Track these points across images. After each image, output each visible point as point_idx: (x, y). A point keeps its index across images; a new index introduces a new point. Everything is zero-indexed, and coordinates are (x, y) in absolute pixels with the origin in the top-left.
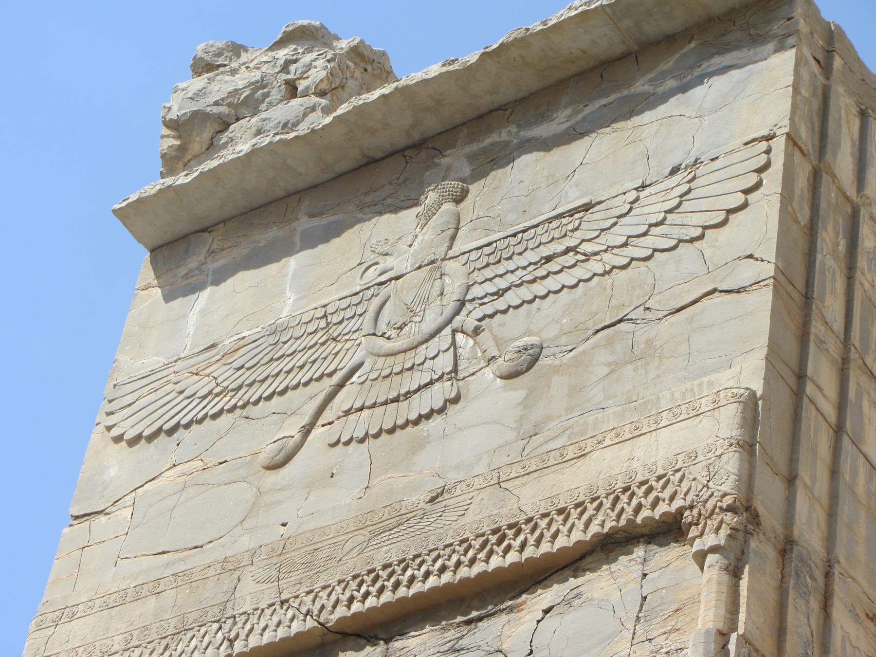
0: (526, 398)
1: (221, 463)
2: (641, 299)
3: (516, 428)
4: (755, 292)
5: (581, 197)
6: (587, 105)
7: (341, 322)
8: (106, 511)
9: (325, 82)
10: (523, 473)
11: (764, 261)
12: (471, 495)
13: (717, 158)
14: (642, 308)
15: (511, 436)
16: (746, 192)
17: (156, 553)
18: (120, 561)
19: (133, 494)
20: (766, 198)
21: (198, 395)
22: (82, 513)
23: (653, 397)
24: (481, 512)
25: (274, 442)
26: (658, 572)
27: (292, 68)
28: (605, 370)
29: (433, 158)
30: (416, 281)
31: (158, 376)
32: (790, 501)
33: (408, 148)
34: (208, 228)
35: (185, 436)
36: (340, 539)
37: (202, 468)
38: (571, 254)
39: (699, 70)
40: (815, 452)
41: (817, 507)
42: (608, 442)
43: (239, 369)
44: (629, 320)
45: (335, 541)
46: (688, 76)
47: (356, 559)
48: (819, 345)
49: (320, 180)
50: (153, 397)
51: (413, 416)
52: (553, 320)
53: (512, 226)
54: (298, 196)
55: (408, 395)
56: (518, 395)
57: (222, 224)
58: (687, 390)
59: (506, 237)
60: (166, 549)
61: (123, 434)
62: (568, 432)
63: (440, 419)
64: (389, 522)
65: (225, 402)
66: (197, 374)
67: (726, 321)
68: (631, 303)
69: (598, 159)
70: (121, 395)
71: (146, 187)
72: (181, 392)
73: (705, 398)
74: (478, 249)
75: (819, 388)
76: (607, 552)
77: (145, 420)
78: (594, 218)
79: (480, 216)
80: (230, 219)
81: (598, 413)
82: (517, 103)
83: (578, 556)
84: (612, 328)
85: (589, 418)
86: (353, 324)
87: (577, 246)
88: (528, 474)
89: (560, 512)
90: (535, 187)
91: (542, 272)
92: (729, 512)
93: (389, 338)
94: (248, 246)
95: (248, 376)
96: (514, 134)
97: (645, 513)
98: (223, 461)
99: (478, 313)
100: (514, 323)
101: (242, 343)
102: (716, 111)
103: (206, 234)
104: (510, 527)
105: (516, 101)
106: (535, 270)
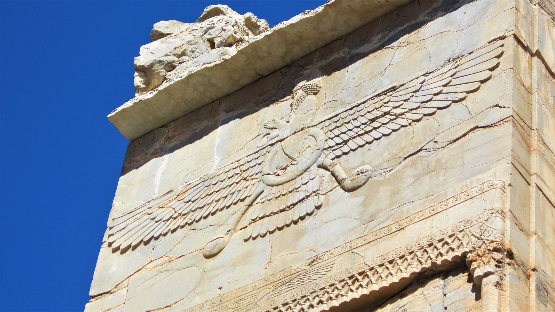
0: (364, 201)
1: (180, 257)
3: (359, 219)
4: (502, 125)
5: (389, 84)
6: (390, 32)
9: (231, 38)
10: (365, 243)
11: (504, 107)
12: (334, 258)
13: (472, 52)
14: (432, 142)
15: (356, 223)
16: (492, 69)
19: (127, 280)
20: (504, 71)
23: (443, 192)
24: (341, 268)
25: (211, 241)
28: (412, 180)
30: (293, 141)
33: (283, 67)
34: (165, 125)
35: (157, 244)
37: (168, 261)
38: (386, 116)
43: (188, 202)
49: (231, 91)
52: (378, 154)
54: (218, 102)
57: (174, 122)
58: (463, 186)
59: (346, 111)
61: (120, 246)
62: (391, 217)
63: (312, 219)
65: (181, 221)
66: (162, 208)
68: (425, 140)
70: (117, 224)
73: (476, 188)
74: (330, 119)
77: (132, 237)
78: (400, 95)
79: (329, 101)
81: (409, 205)
82: (348, 35)
84: (414, 155)
85: (404, 208)
86: (257, 169)
87: (389, 112)
88: (368, 243)
89: (391, 262)
90: (362, 81)
91: (368, 128)
93: (278, 175)
95: (194, 206)
96: (347, 53)
98: (181, 255)
101: (189, 188)
103: (164, 128)
104: (360, 274)
105: (347, 34)
106: (365, 127)
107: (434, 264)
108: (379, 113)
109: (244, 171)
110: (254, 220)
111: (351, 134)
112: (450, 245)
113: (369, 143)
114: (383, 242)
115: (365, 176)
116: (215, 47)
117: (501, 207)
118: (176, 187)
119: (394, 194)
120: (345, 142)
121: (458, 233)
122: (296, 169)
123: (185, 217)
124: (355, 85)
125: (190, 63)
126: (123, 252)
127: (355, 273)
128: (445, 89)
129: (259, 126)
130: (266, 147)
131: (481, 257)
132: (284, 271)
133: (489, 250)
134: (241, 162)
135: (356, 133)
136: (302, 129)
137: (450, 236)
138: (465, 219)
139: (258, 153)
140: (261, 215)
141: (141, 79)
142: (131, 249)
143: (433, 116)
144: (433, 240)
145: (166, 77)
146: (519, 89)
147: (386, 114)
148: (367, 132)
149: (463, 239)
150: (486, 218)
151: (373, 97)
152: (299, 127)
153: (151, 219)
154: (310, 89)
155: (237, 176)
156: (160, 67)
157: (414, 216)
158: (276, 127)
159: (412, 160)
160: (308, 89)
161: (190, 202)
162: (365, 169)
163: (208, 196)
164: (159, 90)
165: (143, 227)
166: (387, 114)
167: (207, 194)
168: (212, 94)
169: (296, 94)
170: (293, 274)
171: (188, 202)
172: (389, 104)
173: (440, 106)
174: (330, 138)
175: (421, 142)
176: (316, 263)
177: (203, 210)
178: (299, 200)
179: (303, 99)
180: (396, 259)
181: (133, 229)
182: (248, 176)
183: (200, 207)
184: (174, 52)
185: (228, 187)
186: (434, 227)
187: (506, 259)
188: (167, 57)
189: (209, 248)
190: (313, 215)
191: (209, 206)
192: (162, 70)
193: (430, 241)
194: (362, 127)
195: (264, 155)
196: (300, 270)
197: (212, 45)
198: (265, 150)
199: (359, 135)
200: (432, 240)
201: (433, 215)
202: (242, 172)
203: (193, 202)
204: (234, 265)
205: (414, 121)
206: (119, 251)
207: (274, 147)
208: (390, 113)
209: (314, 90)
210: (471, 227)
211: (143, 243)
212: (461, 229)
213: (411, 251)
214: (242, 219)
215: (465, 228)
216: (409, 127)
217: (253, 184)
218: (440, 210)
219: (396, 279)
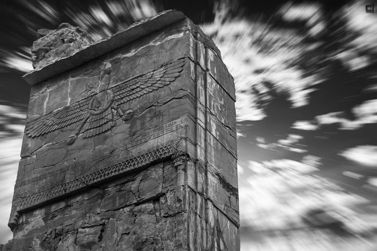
5: (139, 73)
7: (83, 106)
8: (30, 156)
9: (71, 40)
11: (185, 90)
12: (120, 152)
14: (157, 103)
15: (128, 136)
16: (179, 72)
18: (35, 169)
21: (49, 125)
27: (63, 35)
28: (149, 119)
29: (101, 62)
31: (38, 120)
32: (196, 150)
36: (89, 163)
38: (138, 88)
40: (201, 137)
41: (202, 150)
42: (152, 138)
43: (59, 118)
50: (38, 126)
51: (104, 131)
55: (102, 125)
56: (129, 125)
59: (122, 84)
60: (46, 166)
62: (142, 135)
65: (56, 127)
66: (48, 120)
72: (45, 125)
75: (201, 121)
86: (86, 107)
87: (139, 86)
89: (142, 156)
91: (131, 93)
93: (95, 110)
97: (163, 156)
99: (117, 104)
100: (126, 107)
103: (46, 82)
104: (130, 160)
111: (124, 95)
125: (54, 50)
126: (34, 138)
127: (128, 159)
137: (165, 147)
147: (138, 87)
171: (59, 118)
172: (139, 83)
199: (127, 96)
204: (80, 149)
219: (144, 164)
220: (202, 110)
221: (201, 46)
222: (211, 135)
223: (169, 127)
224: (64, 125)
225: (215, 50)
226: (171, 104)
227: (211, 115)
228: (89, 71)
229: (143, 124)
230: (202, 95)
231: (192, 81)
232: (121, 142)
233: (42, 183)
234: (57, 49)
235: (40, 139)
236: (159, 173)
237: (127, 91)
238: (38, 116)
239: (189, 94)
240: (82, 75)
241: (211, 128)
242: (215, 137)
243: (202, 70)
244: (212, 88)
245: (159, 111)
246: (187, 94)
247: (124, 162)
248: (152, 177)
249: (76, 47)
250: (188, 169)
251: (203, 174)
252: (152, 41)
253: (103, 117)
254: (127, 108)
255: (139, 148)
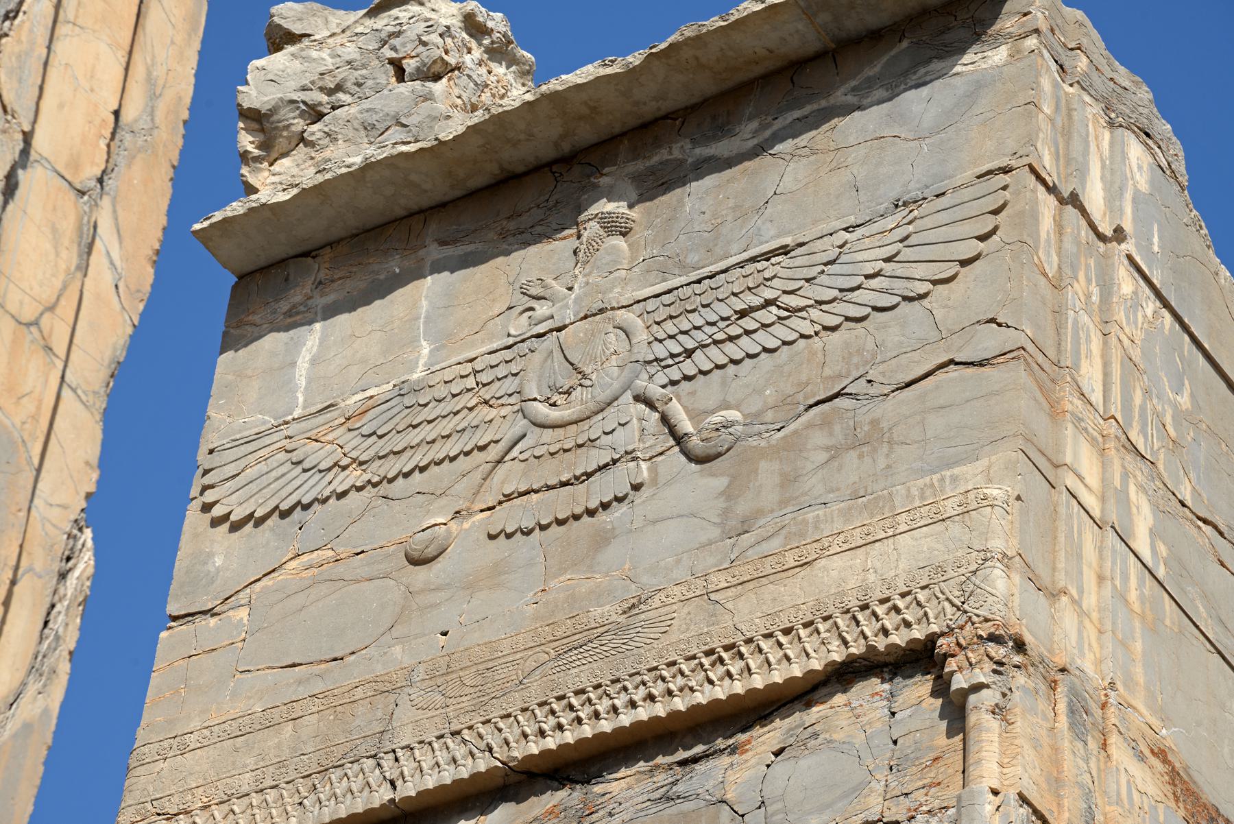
0: (728, 487)
1: (357, 554)
2: (861, 369)
3: (720, 524)
4: (1002, 366)
5: (778, 236)
6: (776, 118)
8: (215, 611)
11: (1009, 327)
12: (675, 607)
13: (943, 194)
14: (863, 380)
15: (715, 533)
17: (284, 665)
19: (248, 590)
20: (1007, 247)
22: (183, 612)
24: (688, 629)
25: (423, 530)
26: (908, 710)
28: (822, 456)
29: (589, 176)
30: (581, 335)
31: (267, 441)
33: (556, 161)
36: (518, 656)
37: (334, 560)
39: (914, 77)
43: (370, 436)
44: (847, 394)
45: (513, 659)
46: (900, 86)
47: (539, 682)
48: (1077, 424)
49: (446, 199)
50: (262, 467)
53: (695, 269)
54: (422, 217)
58: (925, 485)
60: (297, 661)
61: (230, 513)
62: (784, 531)
63: (625, 509)
64: (577, 637)
65: (356, 476)
66: (316, 441)
67: (968, 401)
69: (794, 189)
70: (221, 464)
71: (234, 204)
73: (952, 499)
76: (844, 683)
78: (796, 264)
80: (338, 241)
81: (818, 510)
82: (689, 111)
83: (809, 686)
84: (827, 404)
85: (809, 515)
86: (510, 385)
87: (776, 299)
89: (787, 632)
90: (719, 221)
91: (734, 330)
92: (992, 642)
93: (554, 405)
94: (364, 278)
96: (688, 151)
98: (359, 550)
99: (662, 378)
102: (938, 133)
103: (309, 260)
104: (727, 648)
105: (686, 108)
106: (727, 326)
107: (871, 649)
108: (756, 301)
109: (484, 385)
110: (509, 497)
112: (903, 613)
113: (735, 362)
114: (771, 586)
115: (731, 434)
116: (406, 79)
117: (1002, 548)
118: (342, 398)
119: (788, 480)
120: (689, 353)
121: (918, 590)
122: (589, 396)
123: (364, 467)
124: (706, 229)
125: (354, 110)
126: (236, 527)
127: (716, 644)
128: (889, 268)
129: (511, 286)
130: (528, 338)
131: (965, 648)
132: (573, 620)
133: (980, 637)
134: (478, 365)
135: (710, 337)
136: (602, 311)
137: (903, 595)
138: (931, 563)
139: (510, 350)
140: (522, 488)
141: (251, 139)
142: (252, 523)
143: (864, 324)
144: (868, 597)
145: (305, 135)
146: (1036, 285)
147: (769, 303)
148: (731, 339)
149: (928, 605)
150: (973, 567)
151: (742, 262)
152: (595, 305)
153: (293, 463)
154: (614, 224)
155: (470, 394)
156: (292, 115)
157: (830, 539)
158: (547, 296)
159: (823, 414)
160: (609, 223)
161: (374, 437)
162: (730, 419)
163: (411, 428)
164: (303, 189)
165: (277, 479)
166: (772, 305)
167: (409, 423)
168: (411, 201)
169: (585, 229)
170: (592, 629)
171: (370, 436)
172: (775, 283)
173: (879, 305)
174: (656, 339)
175: (840, 376)
176: (637, 611)
177: (402, 457)
178: (599, 466)
179: (600, 243)
180: (796, 627)
181: (256, 479)
182: (492, 398)
183: (395, 450)
184: (320, 84)
185: (452, 415)
186: (871, 571)
187: (1011, 656)
188: (306, 92)
189: (418, 544)
190: (627, 501)
191: (414, 450)
192: (296, 121)
193: (863, 598)
194: (722, 324)
195: (525, 356)
196: (606, 622)
197: (400, 75)
198: (525, 345)
199: (716, 342)
200: (866, 598)
201: (868, 544)
202: (480, 386)
203: (380, 437)
205: (825, 328)
206: (226, 526)
207: (545, 343)
208: (778, 303)
209: (621, 227)
210: (944, 581)
211: (277, 513)
212: (923, 584)
213: (825, 614)
214: (483, 489)
215: (932, 581)
216: (816, 339)
217: (504, 417)
218: (882, 535)
219: (797, 671)
220: (1086, 429)
221: (1090, 117)
222: (1131, 554)
223: (922, 497)
224: (393, 467)
225: (1156, 143)
226: (937, 387)
227: (1129, 458)
228: (524, 218)
229: (788, 480)
230: (1089, 355)
231: (1043, 280)
232: (678, 561)
233: (278, 746)
234: (366, 104)
235: (272, 530)
236: (870, 723)
237: (713, 318)
238: (264, 423)
239: (1030, 347)
240: (491, 235)
241: (1131, 521)
242: (1150, 564)
243: (1091, 232)
244: (1136, 323)
245: (875, 423)
246: (1019, 345)
247: (694, 657)
248: (835, 736)
249: (459, 102)
250: (1017, 710)
251: (1093, 745)
252: (843, 82)
253: (592, 438)
254: (711, 404)
255: (769, 591)
